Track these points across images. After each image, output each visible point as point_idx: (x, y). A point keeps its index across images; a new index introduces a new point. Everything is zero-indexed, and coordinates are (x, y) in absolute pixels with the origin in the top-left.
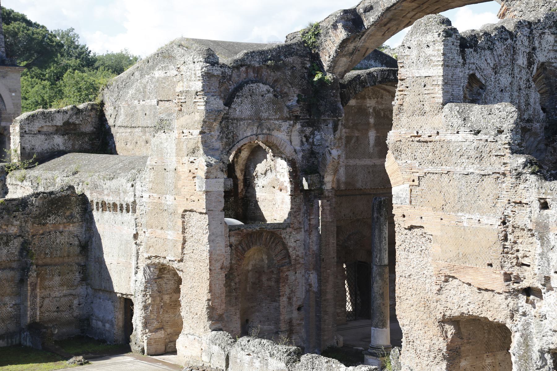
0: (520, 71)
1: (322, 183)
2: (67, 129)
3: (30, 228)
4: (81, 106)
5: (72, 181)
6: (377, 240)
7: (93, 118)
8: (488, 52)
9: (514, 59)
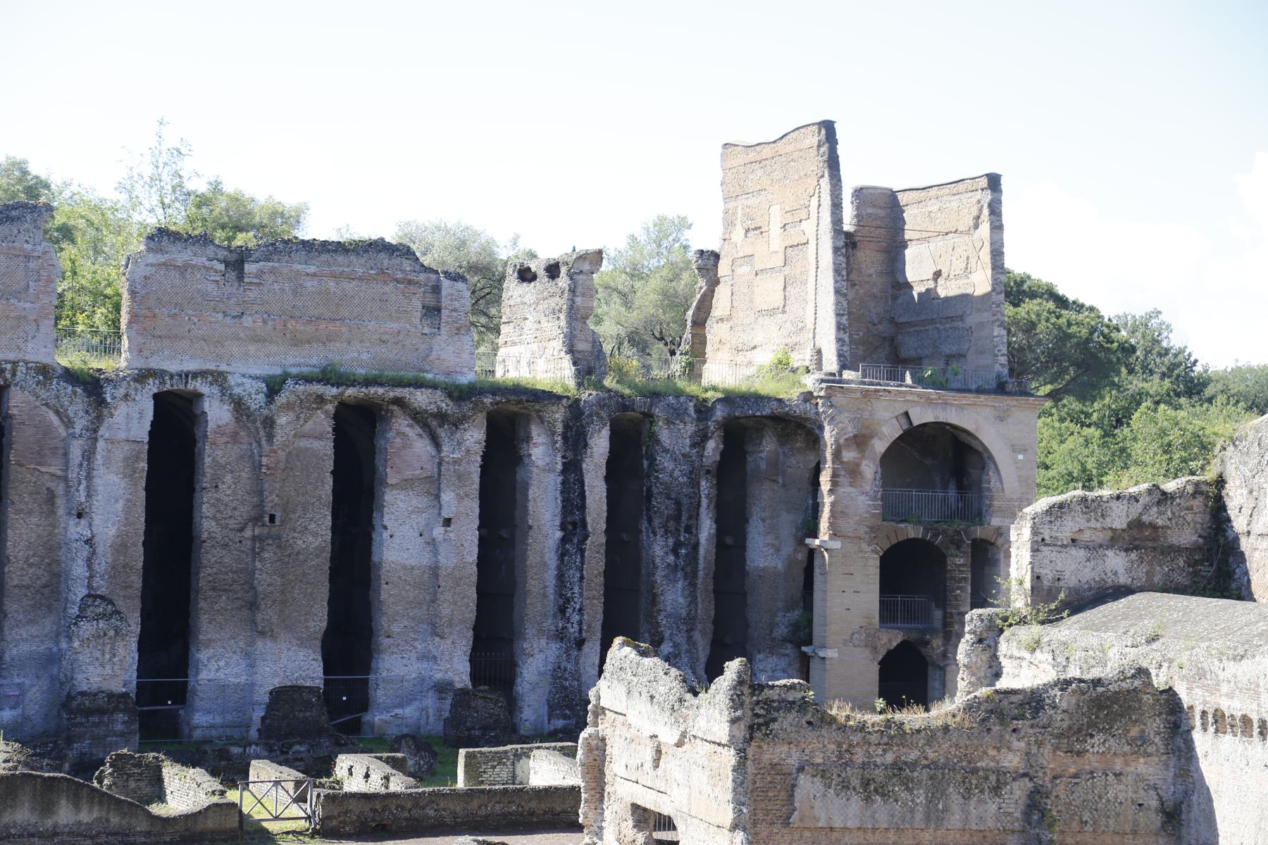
2: (1138, 537)
3: (1050, 760)
4: (1170, 486)
5: (1146, 657)
7: (1197, 515)
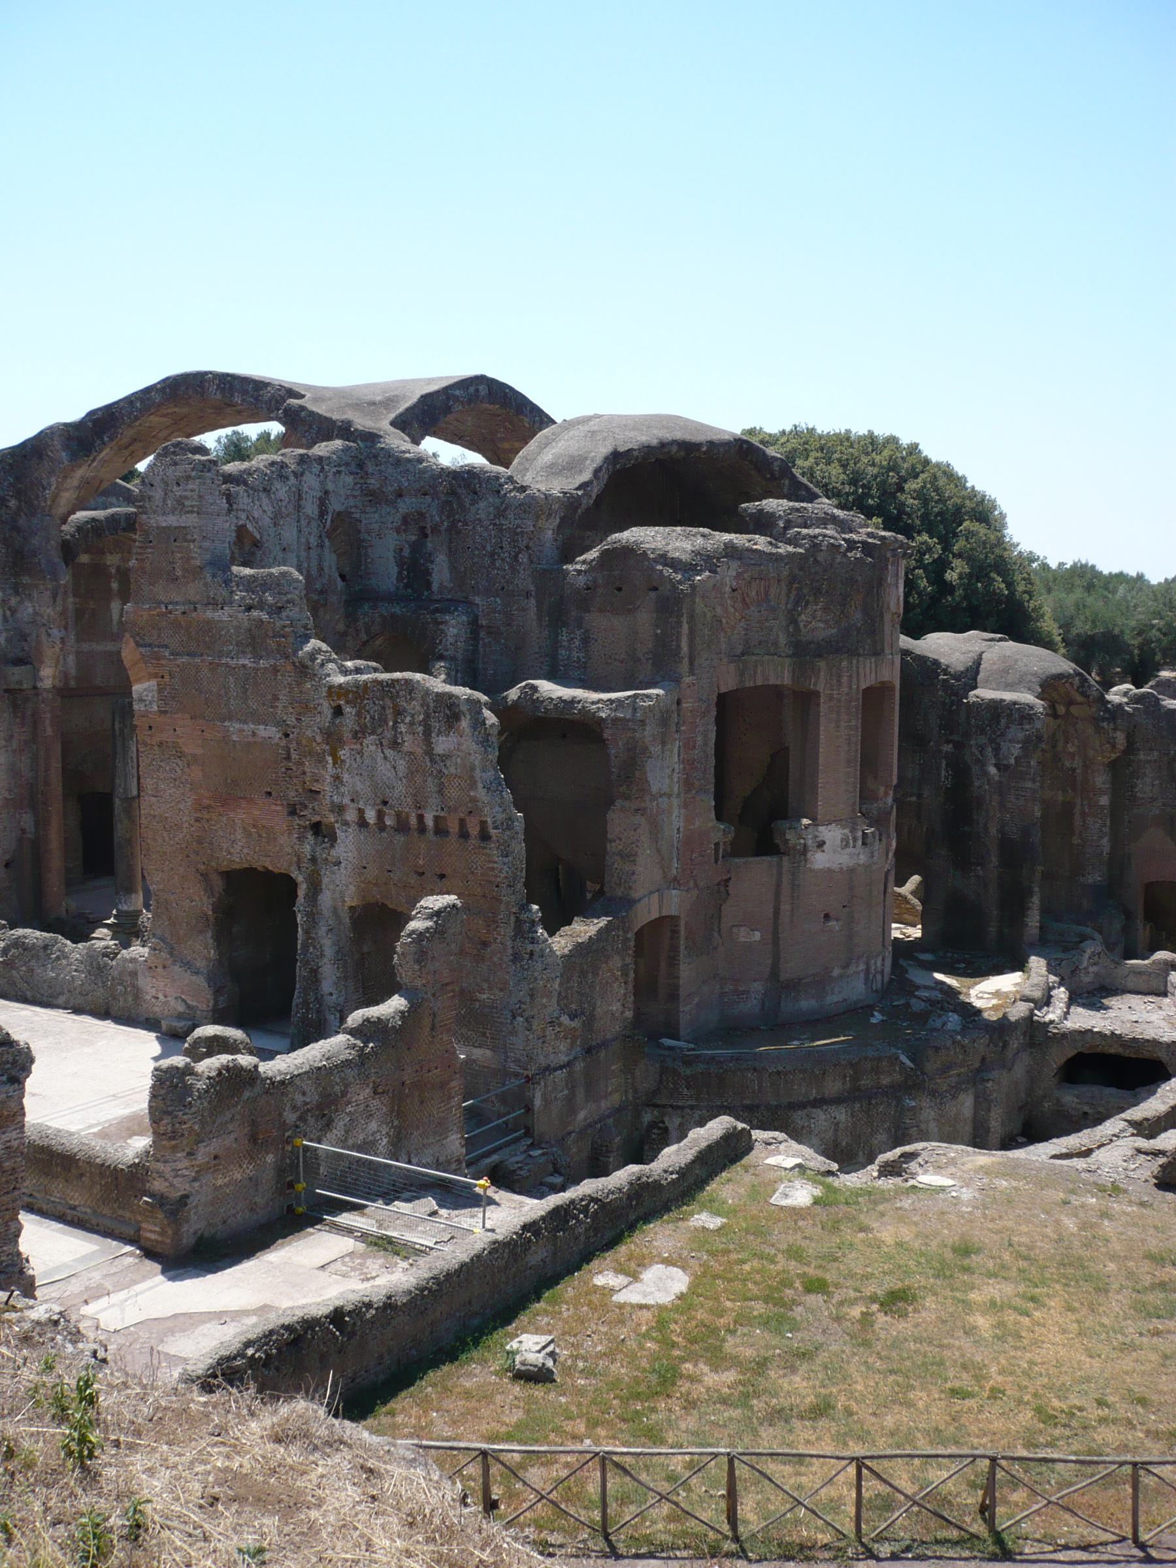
0: (309, 523)
1: (36, 677)
6: (119, 765)
8: (263, 495)
9: (299, 506)
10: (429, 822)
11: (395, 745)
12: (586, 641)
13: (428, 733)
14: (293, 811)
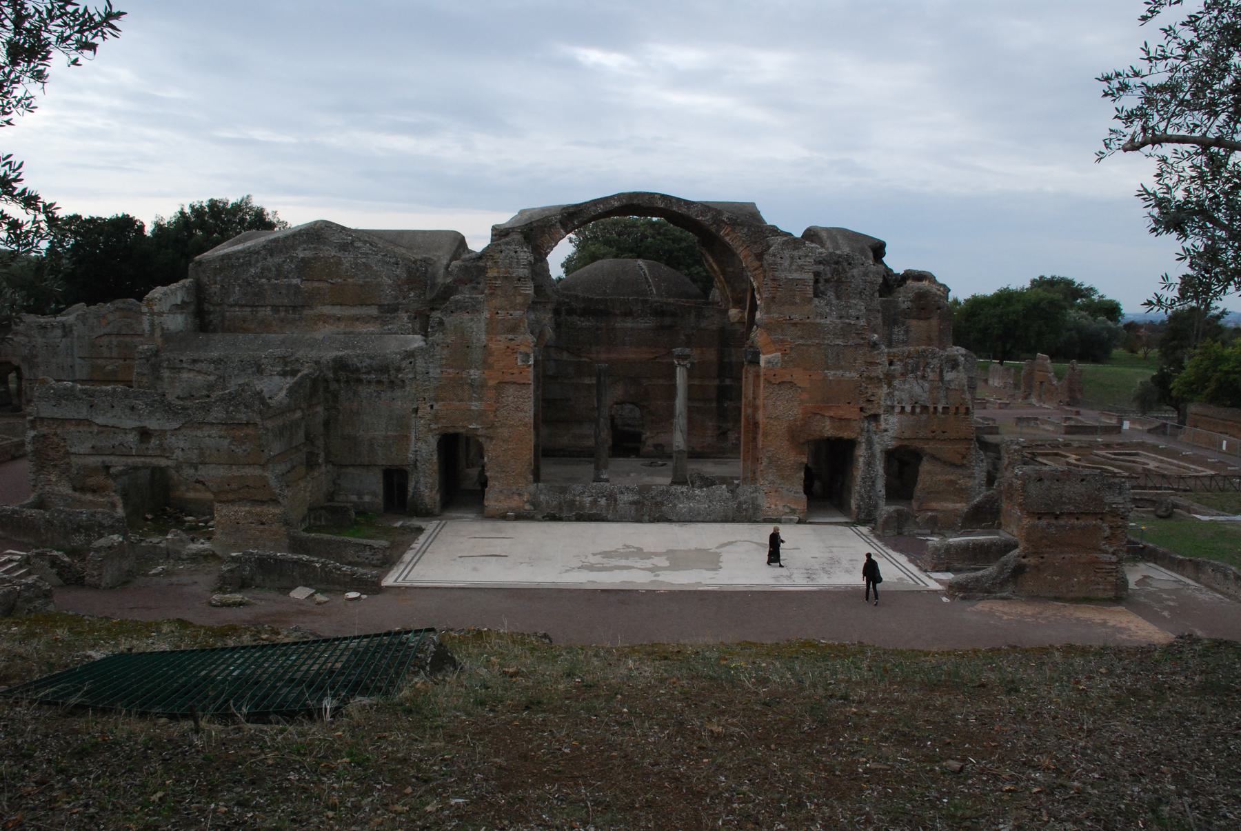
10: (940, 409)
11: (923, 377)
12: (907, 332)
13: (941, 372)
14: (861, 409)
